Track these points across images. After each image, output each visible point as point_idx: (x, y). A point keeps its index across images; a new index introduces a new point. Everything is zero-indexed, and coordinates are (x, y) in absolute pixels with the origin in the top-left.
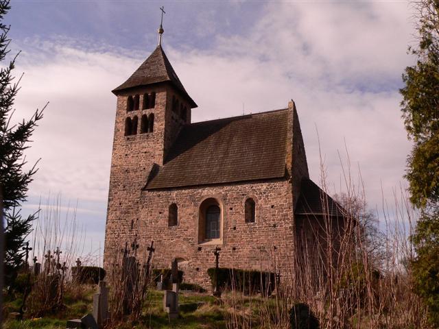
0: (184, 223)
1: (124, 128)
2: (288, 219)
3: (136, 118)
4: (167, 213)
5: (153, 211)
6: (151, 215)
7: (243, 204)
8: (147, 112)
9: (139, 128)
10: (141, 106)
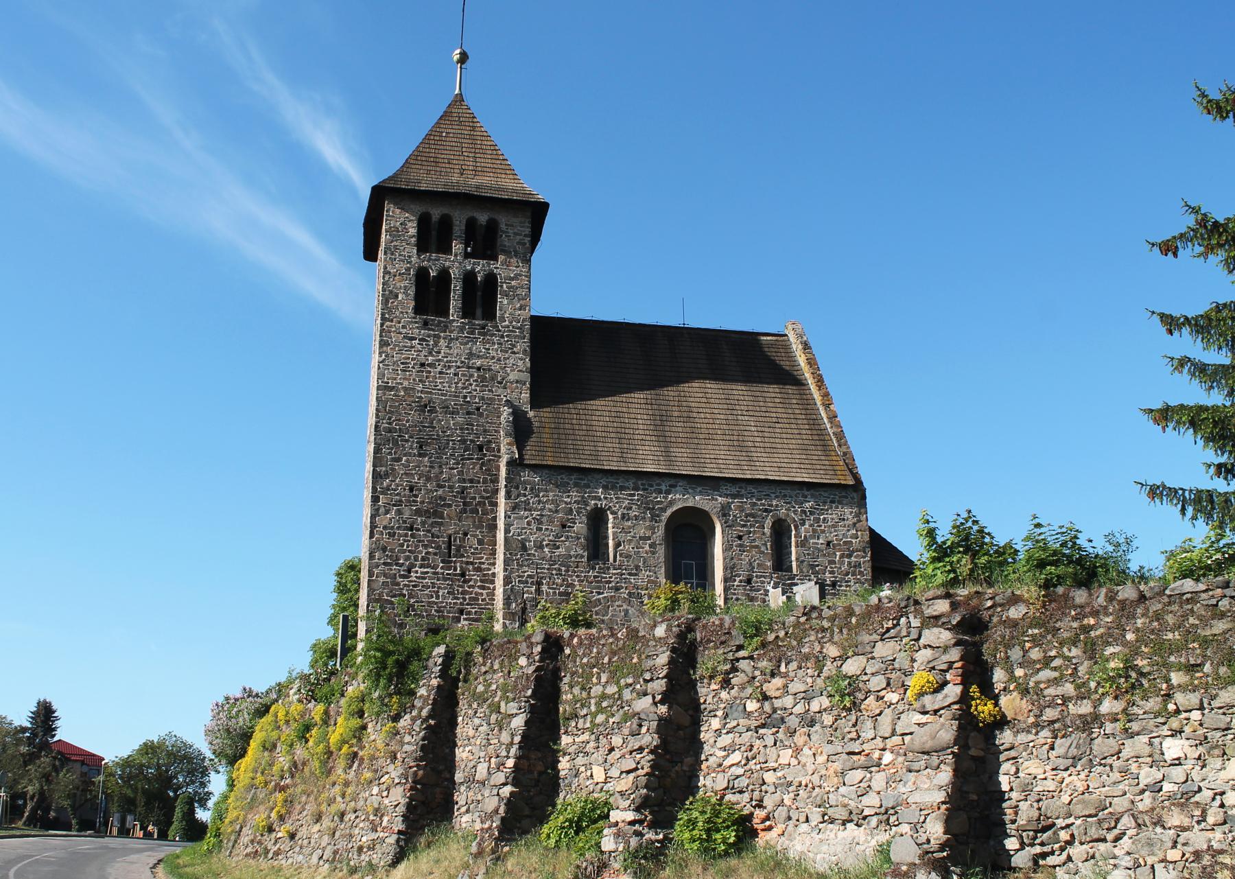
0: (628, 557)
1: (412, 292)
2: (861, 573)
3: (444, 275)
4: (580, 526)
5: (544, 519)
7: (767, 531)
8: (480, 267)
9: (454, 304)
10: (457, 247)
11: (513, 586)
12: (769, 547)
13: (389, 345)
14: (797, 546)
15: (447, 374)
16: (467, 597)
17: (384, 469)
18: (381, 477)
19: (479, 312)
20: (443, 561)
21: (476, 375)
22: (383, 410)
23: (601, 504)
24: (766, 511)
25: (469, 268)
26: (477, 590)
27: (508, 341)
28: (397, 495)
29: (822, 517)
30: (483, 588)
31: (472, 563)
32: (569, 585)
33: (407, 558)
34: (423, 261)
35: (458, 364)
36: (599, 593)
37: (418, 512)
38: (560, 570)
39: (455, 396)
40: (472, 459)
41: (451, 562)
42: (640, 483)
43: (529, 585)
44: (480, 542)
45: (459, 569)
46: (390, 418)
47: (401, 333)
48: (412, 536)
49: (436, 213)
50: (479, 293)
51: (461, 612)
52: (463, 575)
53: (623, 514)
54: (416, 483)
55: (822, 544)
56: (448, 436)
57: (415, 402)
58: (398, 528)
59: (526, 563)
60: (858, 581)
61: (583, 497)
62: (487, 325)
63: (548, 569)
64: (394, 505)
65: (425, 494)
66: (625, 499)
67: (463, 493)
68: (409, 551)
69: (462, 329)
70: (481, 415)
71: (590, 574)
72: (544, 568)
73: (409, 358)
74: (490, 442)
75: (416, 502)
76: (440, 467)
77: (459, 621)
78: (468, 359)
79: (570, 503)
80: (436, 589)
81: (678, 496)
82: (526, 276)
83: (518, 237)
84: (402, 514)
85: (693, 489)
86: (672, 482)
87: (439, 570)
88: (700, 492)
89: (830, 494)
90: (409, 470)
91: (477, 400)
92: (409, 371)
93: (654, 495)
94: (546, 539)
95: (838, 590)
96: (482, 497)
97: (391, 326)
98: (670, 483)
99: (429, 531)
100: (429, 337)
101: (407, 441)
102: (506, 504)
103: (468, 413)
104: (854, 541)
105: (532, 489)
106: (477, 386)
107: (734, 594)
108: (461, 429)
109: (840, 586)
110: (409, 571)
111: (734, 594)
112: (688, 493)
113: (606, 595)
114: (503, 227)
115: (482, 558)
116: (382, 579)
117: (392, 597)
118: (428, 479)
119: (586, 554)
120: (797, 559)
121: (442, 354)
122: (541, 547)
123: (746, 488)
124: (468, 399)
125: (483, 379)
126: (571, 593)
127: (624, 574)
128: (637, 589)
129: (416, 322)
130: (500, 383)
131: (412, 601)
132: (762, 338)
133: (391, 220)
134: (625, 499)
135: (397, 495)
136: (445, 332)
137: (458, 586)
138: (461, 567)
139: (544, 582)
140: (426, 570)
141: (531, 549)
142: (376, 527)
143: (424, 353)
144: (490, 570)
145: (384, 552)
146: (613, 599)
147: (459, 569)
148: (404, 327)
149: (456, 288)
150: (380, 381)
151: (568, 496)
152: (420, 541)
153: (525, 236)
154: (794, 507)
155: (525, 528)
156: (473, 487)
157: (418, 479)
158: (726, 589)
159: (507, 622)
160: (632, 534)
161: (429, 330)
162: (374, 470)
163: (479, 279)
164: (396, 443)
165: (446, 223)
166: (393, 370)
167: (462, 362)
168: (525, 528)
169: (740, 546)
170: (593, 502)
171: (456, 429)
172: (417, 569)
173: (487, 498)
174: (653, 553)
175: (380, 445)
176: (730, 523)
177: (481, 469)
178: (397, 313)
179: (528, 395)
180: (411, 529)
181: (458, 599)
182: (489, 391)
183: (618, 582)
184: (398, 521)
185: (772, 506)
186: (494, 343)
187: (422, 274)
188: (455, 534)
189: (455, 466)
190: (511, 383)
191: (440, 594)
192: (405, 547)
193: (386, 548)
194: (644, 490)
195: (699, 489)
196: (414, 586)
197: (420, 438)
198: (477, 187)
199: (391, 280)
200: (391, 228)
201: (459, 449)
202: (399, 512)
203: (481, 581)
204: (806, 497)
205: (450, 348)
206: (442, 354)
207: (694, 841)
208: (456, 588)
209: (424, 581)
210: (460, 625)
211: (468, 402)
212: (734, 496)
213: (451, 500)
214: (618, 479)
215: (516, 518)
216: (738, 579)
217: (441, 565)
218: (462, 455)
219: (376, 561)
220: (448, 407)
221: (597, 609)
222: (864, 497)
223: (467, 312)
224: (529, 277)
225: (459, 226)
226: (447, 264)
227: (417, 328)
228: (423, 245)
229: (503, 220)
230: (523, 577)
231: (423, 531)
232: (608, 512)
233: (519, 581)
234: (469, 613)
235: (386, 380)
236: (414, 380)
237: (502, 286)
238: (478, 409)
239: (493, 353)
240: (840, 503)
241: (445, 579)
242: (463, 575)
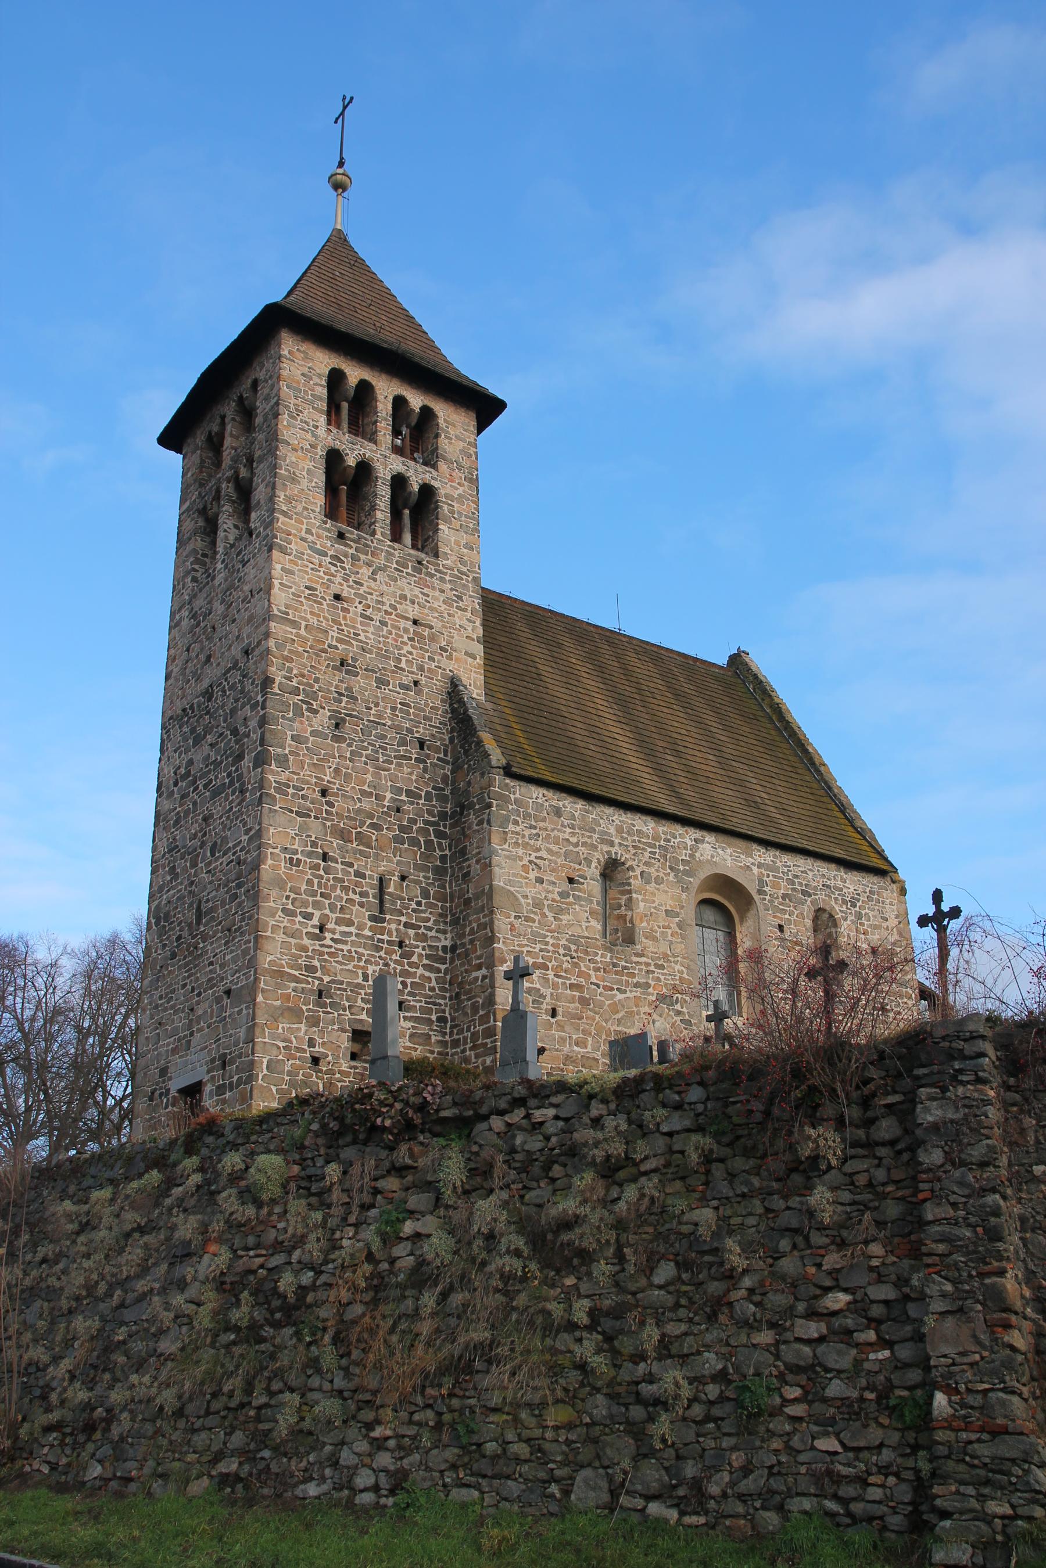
3: (364, 468)
4: (593, 885)
6: (540, 881)
16: (409, 981)
20: (373, 918)
23: (616, 853)
24: (804, 893)
26: (421, 971)
28: (303, 797)
32: (581, 974)
33: (317, 905)
35: (387, 608)
42: (661, 829)
44: (425, 894)
45: (395, 934)
46: (290, 670)
53: (642, 873)
72: (547, 943)
74: (433, 735)
79: (576, 845)
80: (362, 964)
82: (474, 502)
96: (425, 822)
100: (346, 556)
106: (412, 646)
108: (393, 709)
110: (322, 928)
113: (628, 994)
115: (428, 920)
116: (280, 937)
125: (422, 637)
129: (329, 530)
131: (326, 979)
137: (396, 962)
138: (397, 930)
139: (550, 965)
148: (308, 531)
150: (275, 609)
151: (573, 834)
161: (346, 545)
166: (293, 594)
173: (432, 824)
180: (325, 857)
186: (434, 588)
187: (334, 458)
191: (370, 972)
192: (316, 888)
196: (330, 954)
203: (428, 957)
205: (375, 580)
208: (393, 965)
209: (345, 948)
215: (507, 857)
217: (369, 924)
219: (272, 904)
231: (342, 863)
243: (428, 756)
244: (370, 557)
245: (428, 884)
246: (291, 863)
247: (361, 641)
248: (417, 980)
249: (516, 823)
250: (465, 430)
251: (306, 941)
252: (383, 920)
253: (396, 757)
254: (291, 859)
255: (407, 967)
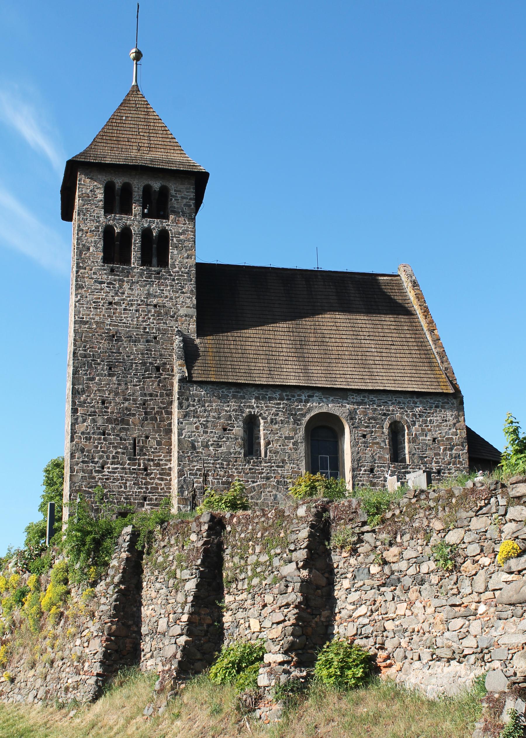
0: (276, 452)
1: (101, 245)
2: (460, 462)
3: (126, 232)
4: (238, 430)
5: (209, 425)
6: (206, 432)
7: (386, 431)
9: (135, 254)
10: (136, 209)
11: (185, 477)
12: (387, 443)
13: (83, 288)
14: (409, 442)
15: (130, 310)
16: (149, 487)
17: (81, 387)
18: (79, 394)
19: (155, 261)
20: (129, 459)
21: (153, 311)
22: (79, 340)
23: (254, 412)
24: (384, 414)
25: (146, 225)
26: (157, 481)
27: (178, 283)
28: (92, 407)
29: (428, 419)
30: (162, 479)
31: (152, 460)
33: (101, 457)
34: (109, 221)
35: (139, 302)
36: (253, 482)
37: (109, 421)
38: (222, 464)
39: (137, 328)
40: (151, 377)
41: (136, 459)
42: (284, 394)
43: (198, 476)
44: (159, 443)
45: (142, 465)
46: (85, 347)
47: (92, 278)
48: (105, 439)
49: (119, 182)
50: (155, 246)
51: (145, 499)
52: (146, 469)
53: (272, 420)
54: (107, 397)
55: (429, 440)
56: (132, 360)
57: (105, 333)
58: (93, 433)
59: (195, 459)
60: (458, 469)
61: (240, 406)
62: (161, 271)
63: (213, 464)
64: (90, 415)
65: (115, 406)
66: (273, 407)
67: (144, 404)
68: (103, 452)
69: (141, 275)
70: (157, 343)
71: (246, 467)
72: (210, 463)
73: (99, 298)
75: (107, 412)
76: (126, 384)
77: (143, 506)
78: (147, 298)
79: (229, 411)
80: (124, 481)
81: (314, 404)
82: (192, 232)
83: (185, 201)
84: (96, 422)
85: (326, 398)
86: (310, 393)
87: (126, 466)
88: (332, 400)
89: (435, 401)
90: (102, 387)
91: (154, 331)
92: (100, 309)
93: (296, 404)
94: (211, 440)
95: (442, 477)
97: (84, 273)
98: (308, 394)
99: (118, 435)
100: (115, 280)
101: (99, 364)
102: (179, 413)
103: (148, 341)
104: (454, 437)
105: (199, 401)
106: (154, 319)
107: (361, 481)
108: (142, 354)
109: (444, 473)
110: (103, 468)
111: (361, 481)
112: (323, 402)
113: (259, 483)
114: (173, 192)
116: (81, 474)
117: (89, 488)
118: (117, 394)
119: (242, 451)
120: (409, 452)
121: (126, 295)
122: (207, 446)
123: (368, 397)
124: (147, 330)
125: (159, 314)
126: (231, 482)
127: (273, 466)
128: (284, 478)
129: (104, 270)
130: (173, 317)
131: (105, 491)
132: (380, 278)
133: (82, 188)
134: (273, 407)
135: (92, 407)
136: (128, 277)
137: (142, 478)
138: (144, 463)
139: (210, 474)
140: (116, 466)
141: (199, 448)
142: (76, 433)
143: (111, 294)
144: (166, 465)
145: (83, 452)
146: (264, 486)
147: (142, 465)
148: (95, 273)
149: (136, 243)
150: (76, 317)
151: (228, 406)
152: (110, 443)
153: (191, 199)
154: (407, 412)
155: (194, 432)
156: (153, 399)
157: (109, 394)
158: (354, 477)
159: (181, 506)
160: (279, 435)
161: (115, 275)
162: (73, 387)
163: (154, 234)
164: (90, 366)
165: (127, 189)
166: (87, 308)
167: (142, 301)
168: (194, 432)
169: (365, 443)
170: (248, 410)
171: (138, 354)
172: (109, 465)
173: (164, 408)
174: (296, 450)
175: (78, 367)
176: (356, 425)
177: (159, 385)
178: (89, 262)
179: (195, 326)
180: (104, 434)
181: (141, 488)
182: (164, 323)
183: (268, 473)
184: (93, 428)
185: (389, 410)
186: (167, 286)
187: (108, 231)
188: (138, 437)
189: (138, 384)
190: (181, 316)
191: (128, 485)
193: (84, 449)
194: (288, 399)
195: (331, 399)
196: (107, 479)
197: (110, 362)
198: (152, 161)
199: (84, 236)
200: (82, 194)
201: (141, 369)
202: (94, 421)
203: (160, 474)
204: (416, 403)
205: (132, 290)
206: (126, 295)
207: (331, 677)
209: (115, 475)
210: (144, 509)
211: (148, 332)
212: (359, 404)
213: (136, 410)
214: (268, 392)
216: (363, 469)
217: (128, 462)
218: (143, 375)
219: (77, 460)
220: (131, 337)
221: (252, 494)
222: (462, 403)
223: (145, 261)
224: (194, 232)
225: (137, 193)
226: (128, 223)
227: (106, 274)
228: (108, 208)
229: (172, 187)
230: (193, 470)
232: (260, 418)
233: (190, 474)
234: (151, 500)
235: (81, 316)
236: (104, 315)
237: (172, 240)
238: (155, 338)
239: (166, 293)
240: (443, 407)
241: (131, 473)
242: (146, 469)
243: (161, 374)
244: (130, 278)
245: (160, 438)
246: (87, 439)
247: (125, 323)
248: (154, 485)
249: (194, 406)
250: (187, 192)
251: (95, 474)
252: (136, 459)
253: (143, 378)
254: (86, 437)
255: (149, 480)
